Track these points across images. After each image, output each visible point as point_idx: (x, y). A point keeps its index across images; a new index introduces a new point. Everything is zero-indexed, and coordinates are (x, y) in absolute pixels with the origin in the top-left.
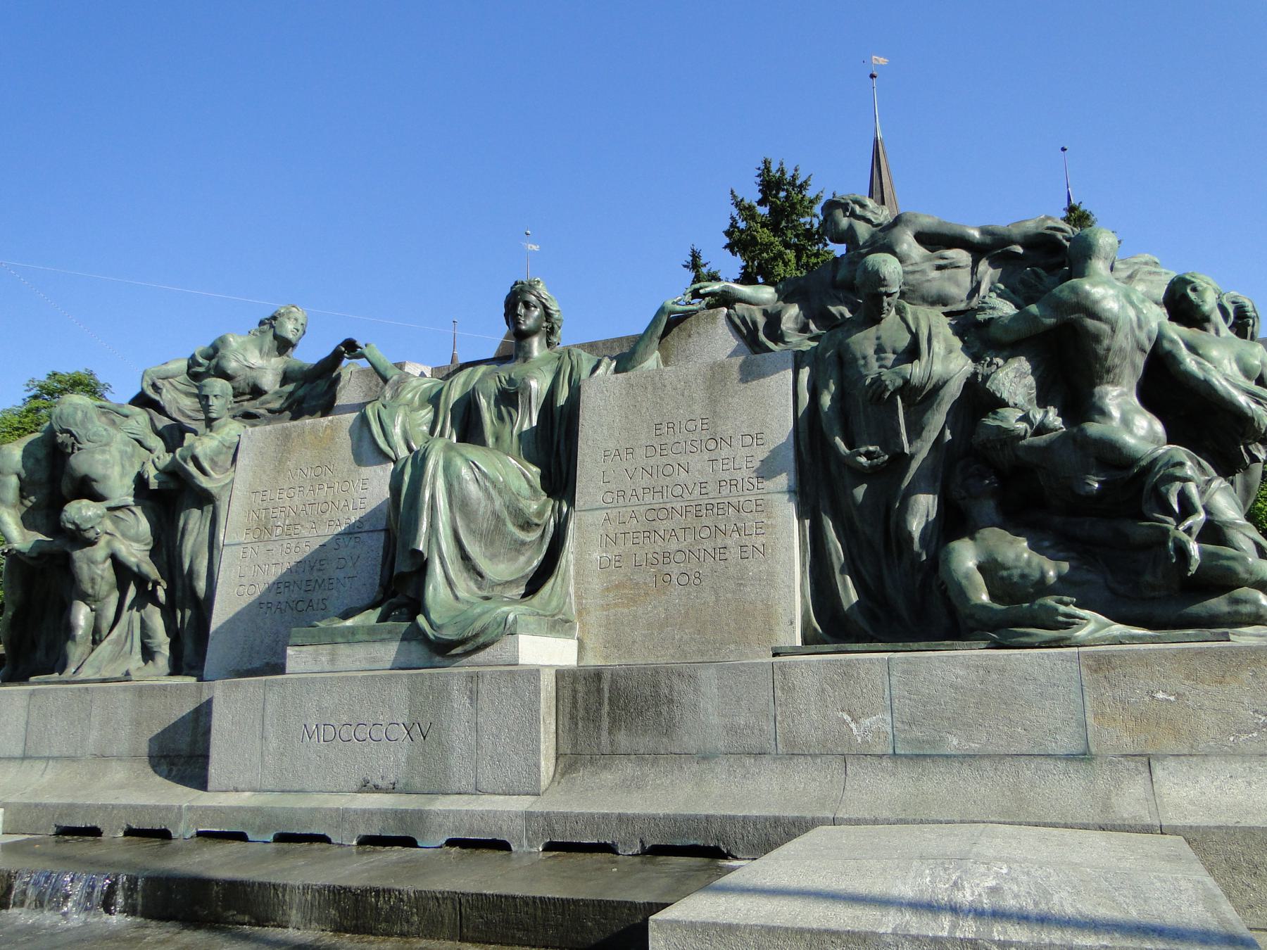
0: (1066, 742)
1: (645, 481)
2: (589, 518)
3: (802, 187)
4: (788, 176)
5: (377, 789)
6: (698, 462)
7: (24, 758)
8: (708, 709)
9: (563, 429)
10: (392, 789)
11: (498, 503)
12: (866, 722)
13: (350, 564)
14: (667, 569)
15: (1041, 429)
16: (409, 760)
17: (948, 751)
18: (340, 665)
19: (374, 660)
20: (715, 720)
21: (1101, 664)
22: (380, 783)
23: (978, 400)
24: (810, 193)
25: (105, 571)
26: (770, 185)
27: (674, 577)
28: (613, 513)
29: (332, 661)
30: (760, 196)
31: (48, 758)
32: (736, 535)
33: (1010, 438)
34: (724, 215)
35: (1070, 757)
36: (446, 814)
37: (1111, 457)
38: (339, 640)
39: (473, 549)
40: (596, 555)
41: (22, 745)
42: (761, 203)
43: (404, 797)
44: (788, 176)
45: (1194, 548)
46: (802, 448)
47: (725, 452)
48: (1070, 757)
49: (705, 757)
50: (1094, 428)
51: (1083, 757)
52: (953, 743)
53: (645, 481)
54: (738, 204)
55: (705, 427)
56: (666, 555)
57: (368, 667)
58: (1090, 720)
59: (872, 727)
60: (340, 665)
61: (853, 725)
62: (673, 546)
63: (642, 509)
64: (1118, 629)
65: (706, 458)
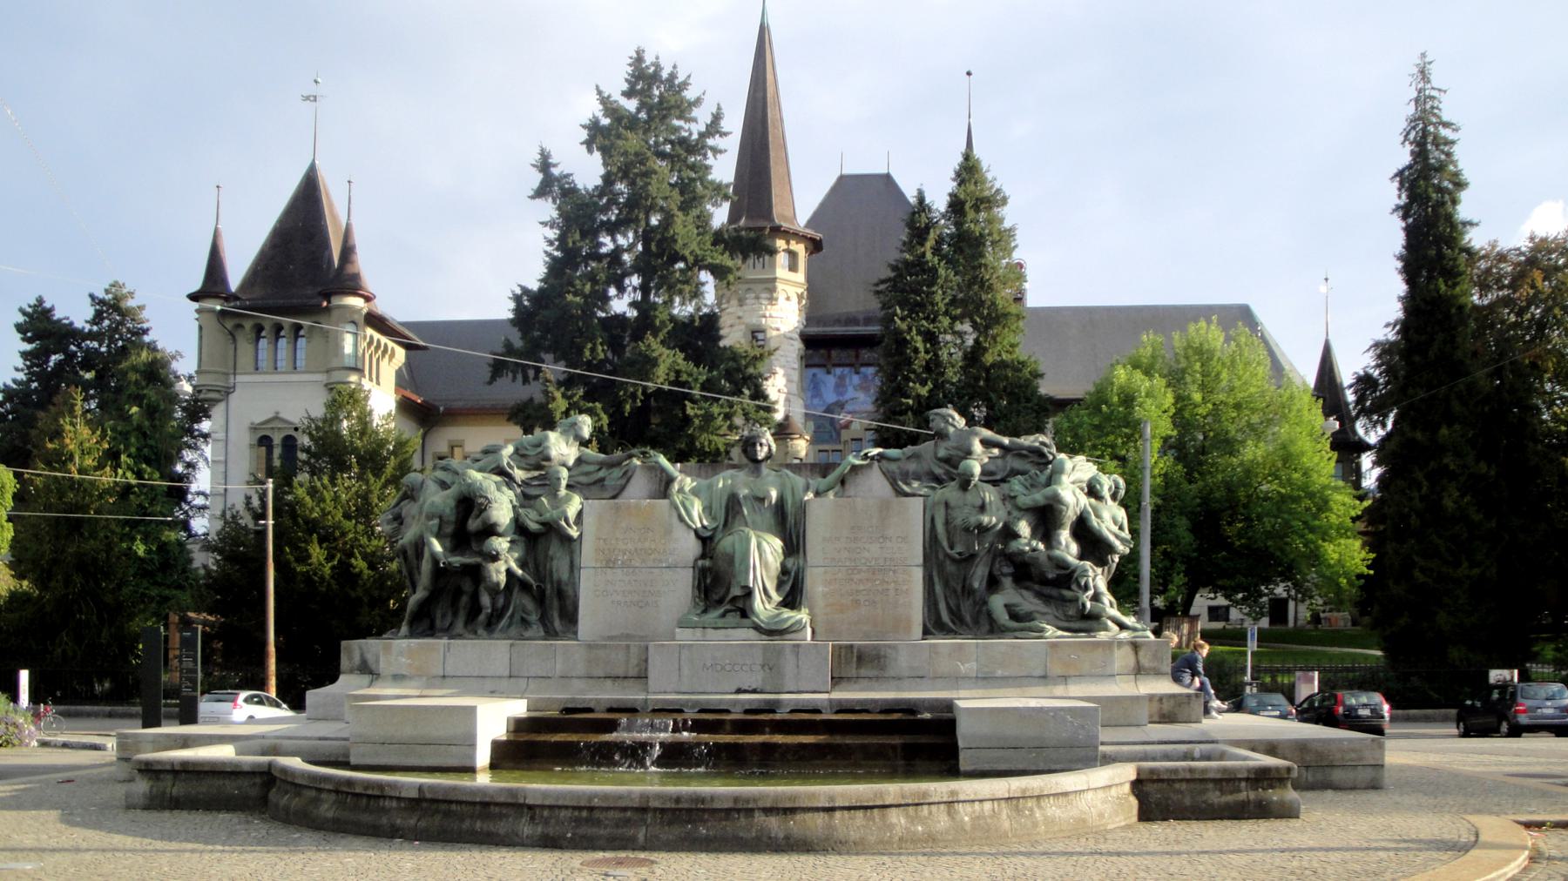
2: (816, 570)
3: (685, 85)
4: (665, 75)
6: (874, 549)
8: (902, 662)
15: (1034, 550)
21: (1054, 645)
23: (1009, 534)
24: (690, 94)
25: (502, 579)
26: (643, 77)
30: (625, 86)
33: (1023, 553)
34: (592, 108)
37: (1061, 565)
42: (628, 94)
44: (665, 75)
45: (1088, 605)
47: (888, 544)
50: (1057, 552)
54: (605, 101)
64: (1060, 633)
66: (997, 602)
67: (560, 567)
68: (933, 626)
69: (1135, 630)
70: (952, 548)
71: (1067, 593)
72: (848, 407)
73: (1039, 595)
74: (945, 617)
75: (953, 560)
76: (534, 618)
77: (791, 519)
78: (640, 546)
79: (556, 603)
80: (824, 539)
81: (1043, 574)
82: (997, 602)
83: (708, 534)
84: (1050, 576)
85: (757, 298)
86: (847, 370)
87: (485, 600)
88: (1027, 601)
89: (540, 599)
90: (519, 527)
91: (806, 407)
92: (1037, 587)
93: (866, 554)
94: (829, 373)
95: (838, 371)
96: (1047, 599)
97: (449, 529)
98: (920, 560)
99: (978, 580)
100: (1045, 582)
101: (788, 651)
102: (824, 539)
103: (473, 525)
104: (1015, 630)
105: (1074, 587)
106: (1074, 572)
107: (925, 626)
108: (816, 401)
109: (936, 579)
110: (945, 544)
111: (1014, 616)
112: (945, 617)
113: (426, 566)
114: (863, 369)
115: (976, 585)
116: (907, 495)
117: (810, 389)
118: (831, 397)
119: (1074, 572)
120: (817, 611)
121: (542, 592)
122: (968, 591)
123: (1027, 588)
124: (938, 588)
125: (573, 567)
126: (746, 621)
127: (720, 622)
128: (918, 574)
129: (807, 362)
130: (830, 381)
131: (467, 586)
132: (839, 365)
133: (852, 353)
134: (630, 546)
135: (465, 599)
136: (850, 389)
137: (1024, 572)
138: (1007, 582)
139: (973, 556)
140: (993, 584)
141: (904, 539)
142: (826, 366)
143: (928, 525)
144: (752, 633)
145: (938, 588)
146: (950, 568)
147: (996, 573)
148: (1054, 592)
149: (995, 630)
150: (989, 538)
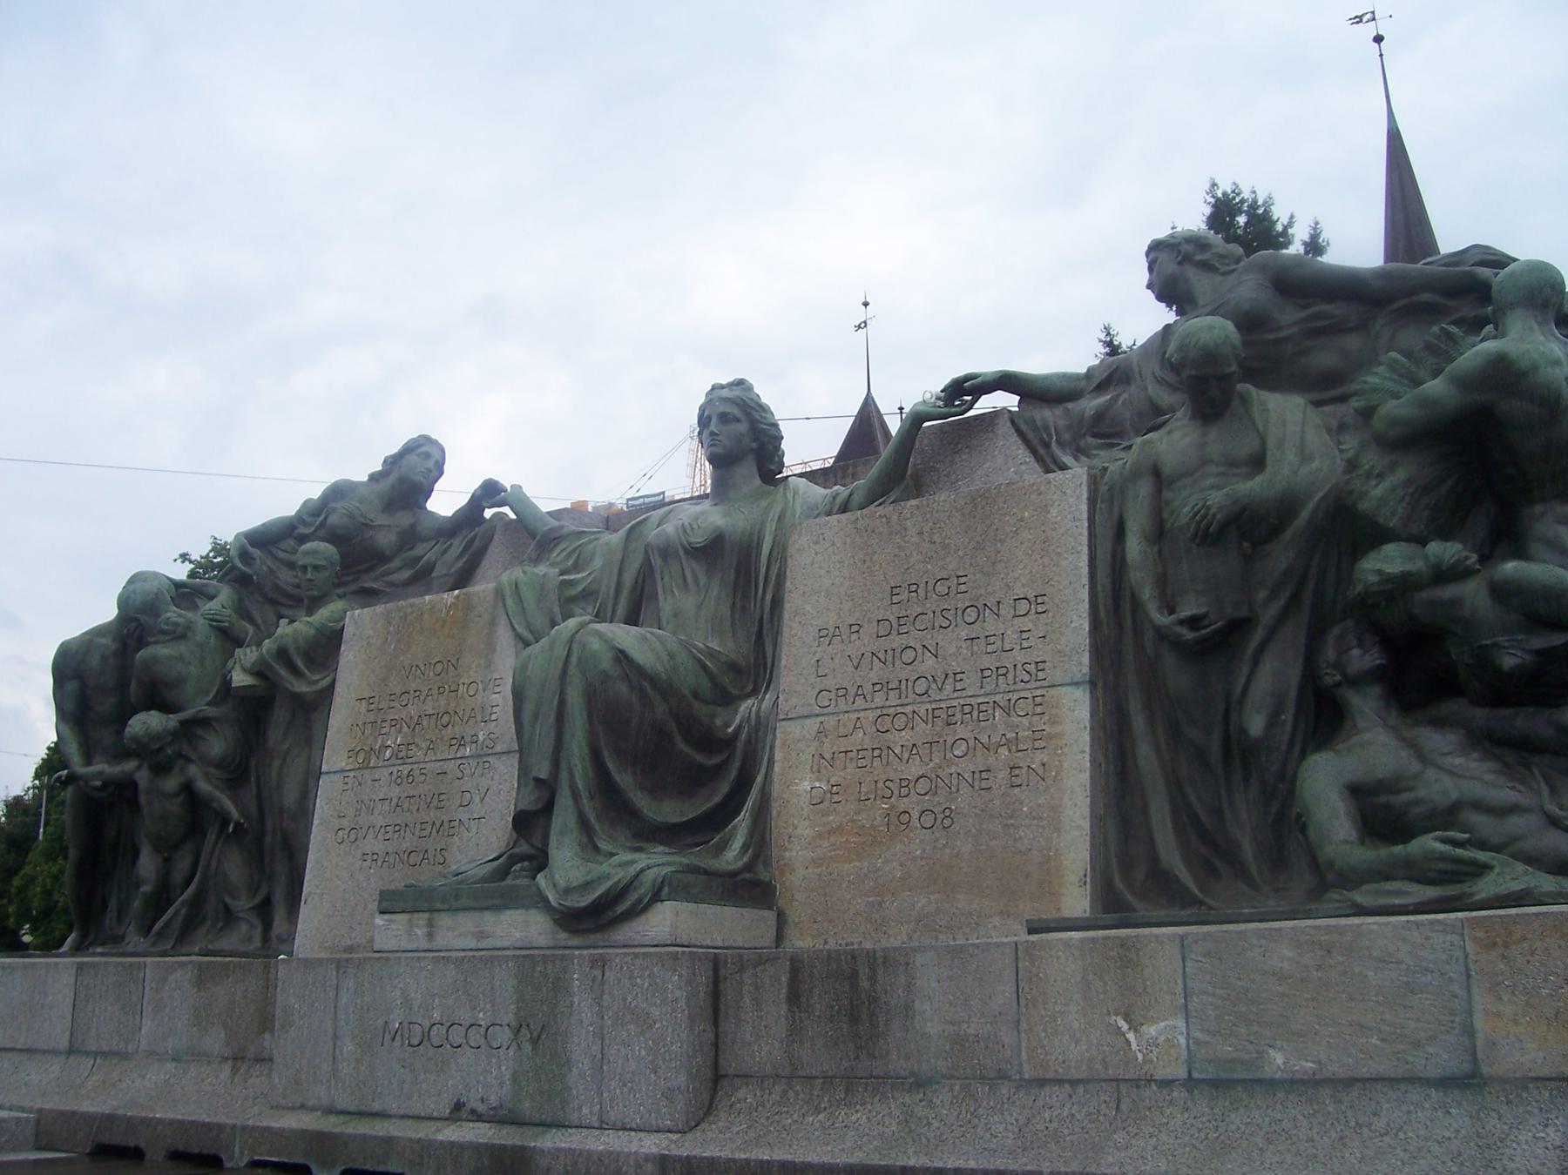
0: (1442, 1058)
1: (876, 672)
5: (477, 1116)
7: (71, 1051)
9: (769, 597)
11: (660, 709)
12: (1151, 1030)
13: (477, 800)
14: (904, 804)
16: (515, 1079)
17: (1268, 1072)
18: (441, 940)
19: (481, 935)
20: (933, 1028)
22: (480, 1108)
27: (915, 815)
28: (830, 722)
29: (430, 935)
31: (95, 1054)
32: (1003, 751)
35: (1446, 1083)
36: (557, 1153)
38: (438, 905)
39: (624, 779)
40: (806, 785)
41: (67, 1035)
43: (506, 1130)
46: (1102, 614)
47: (991, 625)
48: (1446, 1083)
49: (920, 1083)
51: (1468, 1081)
52: (1277, 1061)
53: (876, 672)
55: (962, 588)
57: (473, 945)
58: (1479, 1023)
59: (1162, 1039)
60: (441, 940)
61: (1131, 1036)
62: (915, 769)
63: (872, 715)
65: (964, 635)
66: (1324, 781)
68: (1134, 884)
73: (1490, 742)
74: (1171, 856)
75: (1177, 645)
76: (242, 904)
81: (1484, 659)
82: (1324, 781)
84: (1508, 662)
88: (1446, 766)
89: (258, 859)
92: (1480, 715)
96: (1514, 751)
102: (824, 634)
109: (1139, 722)
110: (1147, 594)
112: (1171, 856)
115: (1256, 724)
122: (1239, 754)
123: (1438, 723)
124: (1146, 755)
125: (313, 775)
128: (1075, 712)
138: (1365, 705)
139: (1238, 628)
140: (1323, 717)
141: (1037, 603)
143: (1104, 549)
145: (1146, 755)
146: (1177, 676)
147: (1331, 678)
149: (1327, 884)
150: (1280, 557)
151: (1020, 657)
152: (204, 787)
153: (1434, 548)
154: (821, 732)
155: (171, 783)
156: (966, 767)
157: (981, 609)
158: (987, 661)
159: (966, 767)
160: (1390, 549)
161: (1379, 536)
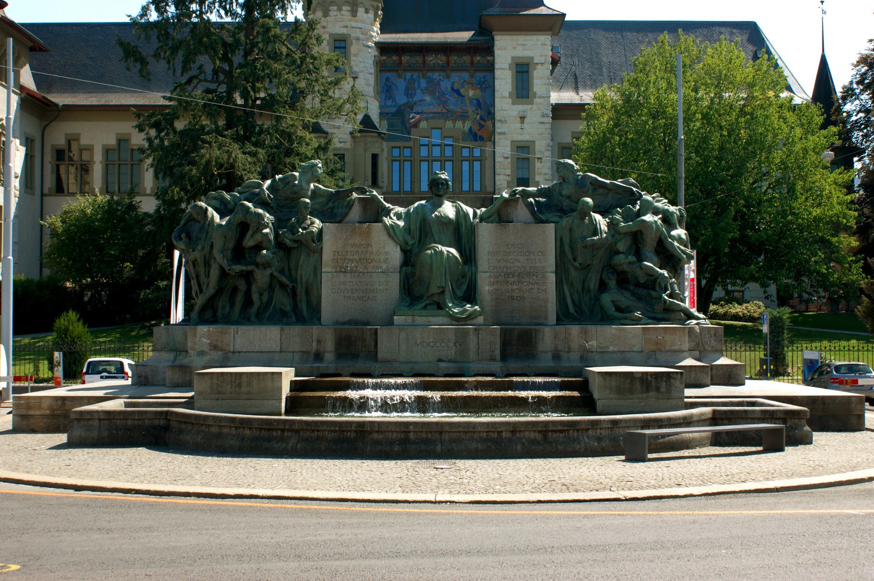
2: (483, 275)
10: (450, 361)
40: (487, 288)
56: (513, 290)
67: (304, 272)
69: (698, 318)
70: (575, 260)
71: (654, 294)
72: (417, 108)
73: (633, 294)
77: (464, 240)
78: (363, 256)
79: (304, 298)
80: (489, 253)
82: (606, 299)
83: (409, 248)
85: (340, 10)
86: (416, 75)
87: (255, 297)
90: (280, 244)
91: (381, 107)
93: (517, 264)
94: (400, 76)
95: (408, 75)
96: (639, 298)
97: (231, 245)
98: (553, 268)
99: (593, 284)
100: (638, 285)
101: (471, 333)
103: (249, 242)
104: (620, 319)
105: (657, 288)
106: (656, 278)
107: (558, 315)
108: (389, 102)
109: (564, 282)
111: (619, 309)
113: (215, 272)
114: (430, 74)
115: (592, 287)
116: (543, 222)
117: (385, 90)
118: (402, 100)
119: (656, 278)
120: (485, 303)
121: (294, 289)
125: (317, 271)
126: (441, 312)
127: (424, 312)
128: (552, 278)
129: (381, 68)
130: (401, 84)
131: (242, 286)
132: (409, 71)
133: (419, 59)
134: (356, 257)
135: (239, 298)
136: (419, 91)
137: (624, 281)
140: (603, 286)
142: (398, 68)
144: (446, 320)
148: (644, 292)
149: (606, 319)
151: (539, 264)
152: (276, 274)
153: (630, 257)
154: (490, 276)
155: (268, 272)
156: (527, 288)
157: (530, 253)
158: (532, 265)
159: (527, 288)
160: (622, 256)
161: (618, 253)
